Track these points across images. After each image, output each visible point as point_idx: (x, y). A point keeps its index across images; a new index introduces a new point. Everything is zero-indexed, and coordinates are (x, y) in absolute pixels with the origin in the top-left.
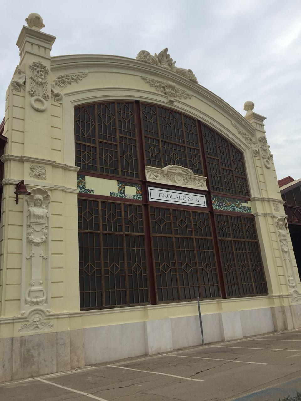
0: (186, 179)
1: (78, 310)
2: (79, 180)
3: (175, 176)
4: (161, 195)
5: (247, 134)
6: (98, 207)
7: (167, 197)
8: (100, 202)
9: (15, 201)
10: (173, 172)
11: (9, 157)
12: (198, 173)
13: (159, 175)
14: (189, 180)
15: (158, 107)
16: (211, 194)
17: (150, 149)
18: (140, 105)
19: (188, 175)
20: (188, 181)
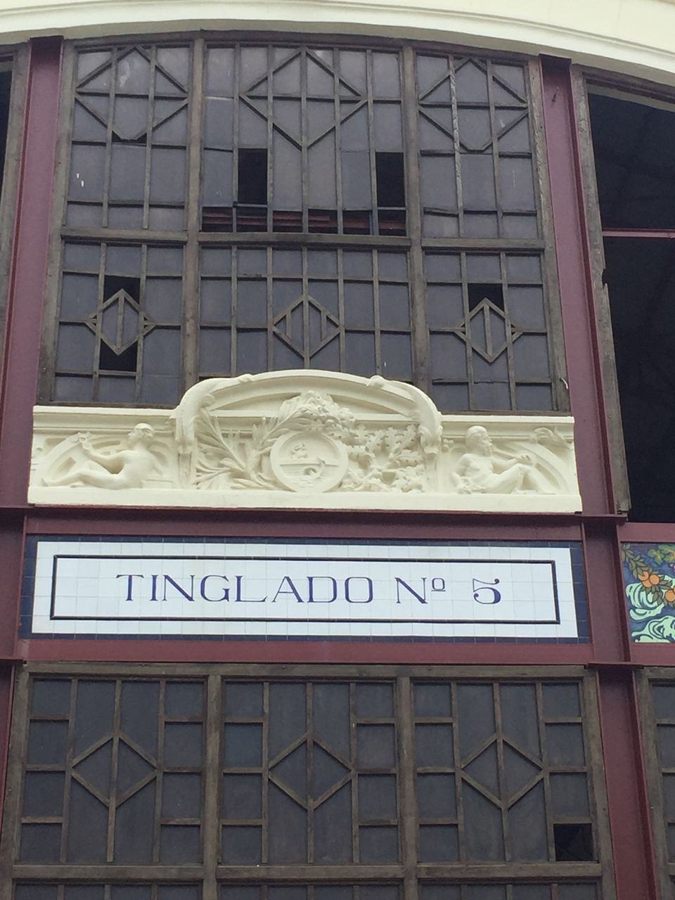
0: (383, 449)
3: (281, 441)
4: (142, 588)
10: (258, 422)
20: (406, 464)
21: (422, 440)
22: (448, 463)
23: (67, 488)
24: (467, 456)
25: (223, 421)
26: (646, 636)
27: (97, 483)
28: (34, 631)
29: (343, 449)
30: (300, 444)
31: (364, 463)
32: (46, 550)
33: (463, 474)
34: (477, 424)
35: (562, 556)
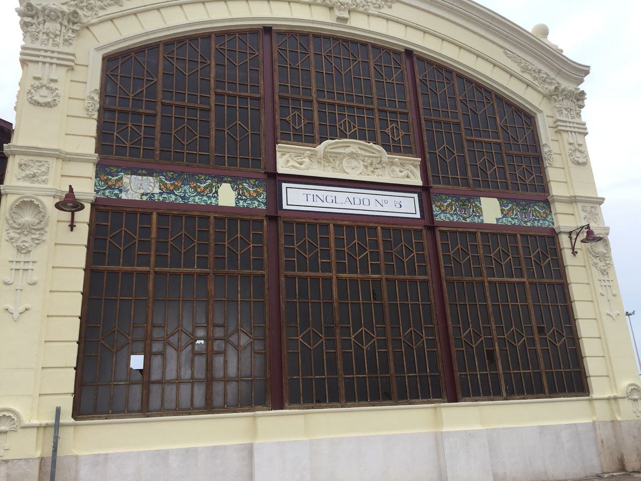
0: (371, 164)
1: (72, 421)
2: (207, 184)
3: (345, 160)
4: (310, 198)
5: (545, 69)
6: (328, 233)
7: (362, 202)
8: (331, 226)
9: (69, 226)
10: (339, 153)
11: (11, 149)
12: (401, 152)
13: (307, 160)
14: (378, 166)
15: (371, 45)
16: (431, 190)
17: (390, 127)
18: (415, 59)
19: (375, 157)
20: (377, 169)
21: (382, 162)
22: (388, 170)
23: (289, 169)
24: (393, 167)
25: (330, 152)
26: (437, 219)
27: (297, 168)
28: (284, 208)
29: (362, 163)
30: (350, 160)
31: (366, 167)
32: (284, 185)
33: (392, 172)
34: (397, 158)
35: (416, 196)
